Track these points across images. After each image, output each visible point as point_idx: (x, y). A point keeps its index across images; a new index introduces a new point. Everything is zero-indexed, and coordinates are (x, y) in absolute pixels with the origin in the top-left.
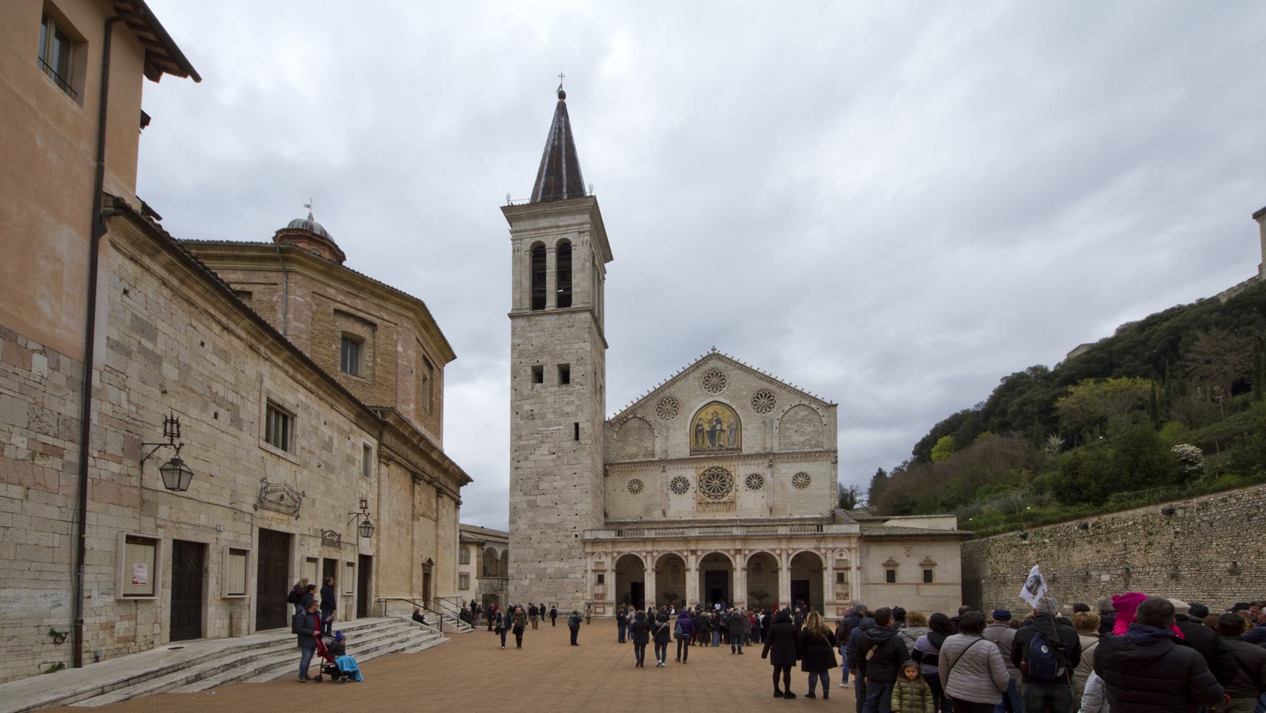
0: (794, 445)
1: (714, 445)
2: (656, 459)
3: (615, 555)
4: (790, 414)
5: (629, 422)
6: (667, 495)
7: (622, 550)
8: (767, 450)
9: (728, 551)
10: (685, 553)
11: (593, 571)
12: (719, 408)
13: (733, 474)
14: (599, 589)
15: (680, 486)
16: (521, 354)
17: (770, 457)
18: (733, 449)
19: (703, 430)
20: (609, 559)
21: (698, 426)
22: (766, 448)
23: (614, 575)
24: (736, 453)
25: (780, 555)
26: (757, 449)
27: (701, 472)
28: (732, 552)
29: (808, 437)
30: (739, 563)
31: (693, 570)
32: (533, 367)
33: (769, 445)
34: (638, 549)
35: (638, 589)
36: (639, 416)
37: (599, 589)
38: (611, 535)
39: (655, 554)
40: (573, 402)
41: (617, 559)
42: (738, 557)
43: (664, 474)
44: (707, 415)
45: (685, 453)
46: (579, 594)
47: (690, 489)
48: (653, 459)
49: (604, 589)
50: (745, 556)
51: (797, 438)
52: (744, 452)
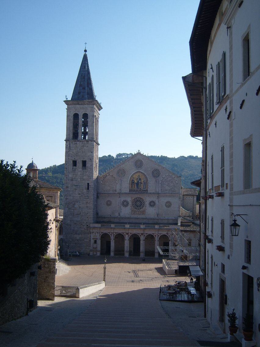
0: (166, 190)
1: (138, 188)
2: (117, 192)
3: (101, 233)
4: (165, 178)
5: (107, 177)
6: (121, 206)
7: (103, 231)
8: (157, 192)
9: (139, 234)
10: (125, 234)
11: (93, 239)
12: (140, 174)
13: (145, 200)
14: (95, 245)
15: (125, 204)
16: (69, 156)
17: (158, 194)
18: (145, 190)
19: (134, 182)
20: (99, 235)
21: (132, 180)
22: (156, 191)
23: (100, 240)
24: (145, 192)
25: (156, 236)
26: (153, 191)
27: (133, 199)
28: (140, 234)
29: (171, 188)
30: (142, 238)
31: (127, 240)
32: (73, 161)
33: (157, 190)
34: (109, 232)
35: (109, 243)
36: (111, 175)
37: (95, 245)
38: (99, 225)
39: (114, 233)
40: (87, 175)
41: (101, 235)
42: (142, 236)
43: (120, 199)
44: (136, 176)
45: (128, 191)
46: (87, 247)
47: (129, 205)
48: (115, 192)
49: (96, 246)
50: (144, 235)
51: (167, 188)
52: (149, 192)
